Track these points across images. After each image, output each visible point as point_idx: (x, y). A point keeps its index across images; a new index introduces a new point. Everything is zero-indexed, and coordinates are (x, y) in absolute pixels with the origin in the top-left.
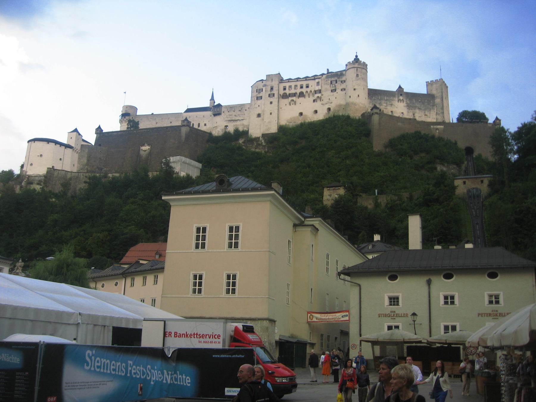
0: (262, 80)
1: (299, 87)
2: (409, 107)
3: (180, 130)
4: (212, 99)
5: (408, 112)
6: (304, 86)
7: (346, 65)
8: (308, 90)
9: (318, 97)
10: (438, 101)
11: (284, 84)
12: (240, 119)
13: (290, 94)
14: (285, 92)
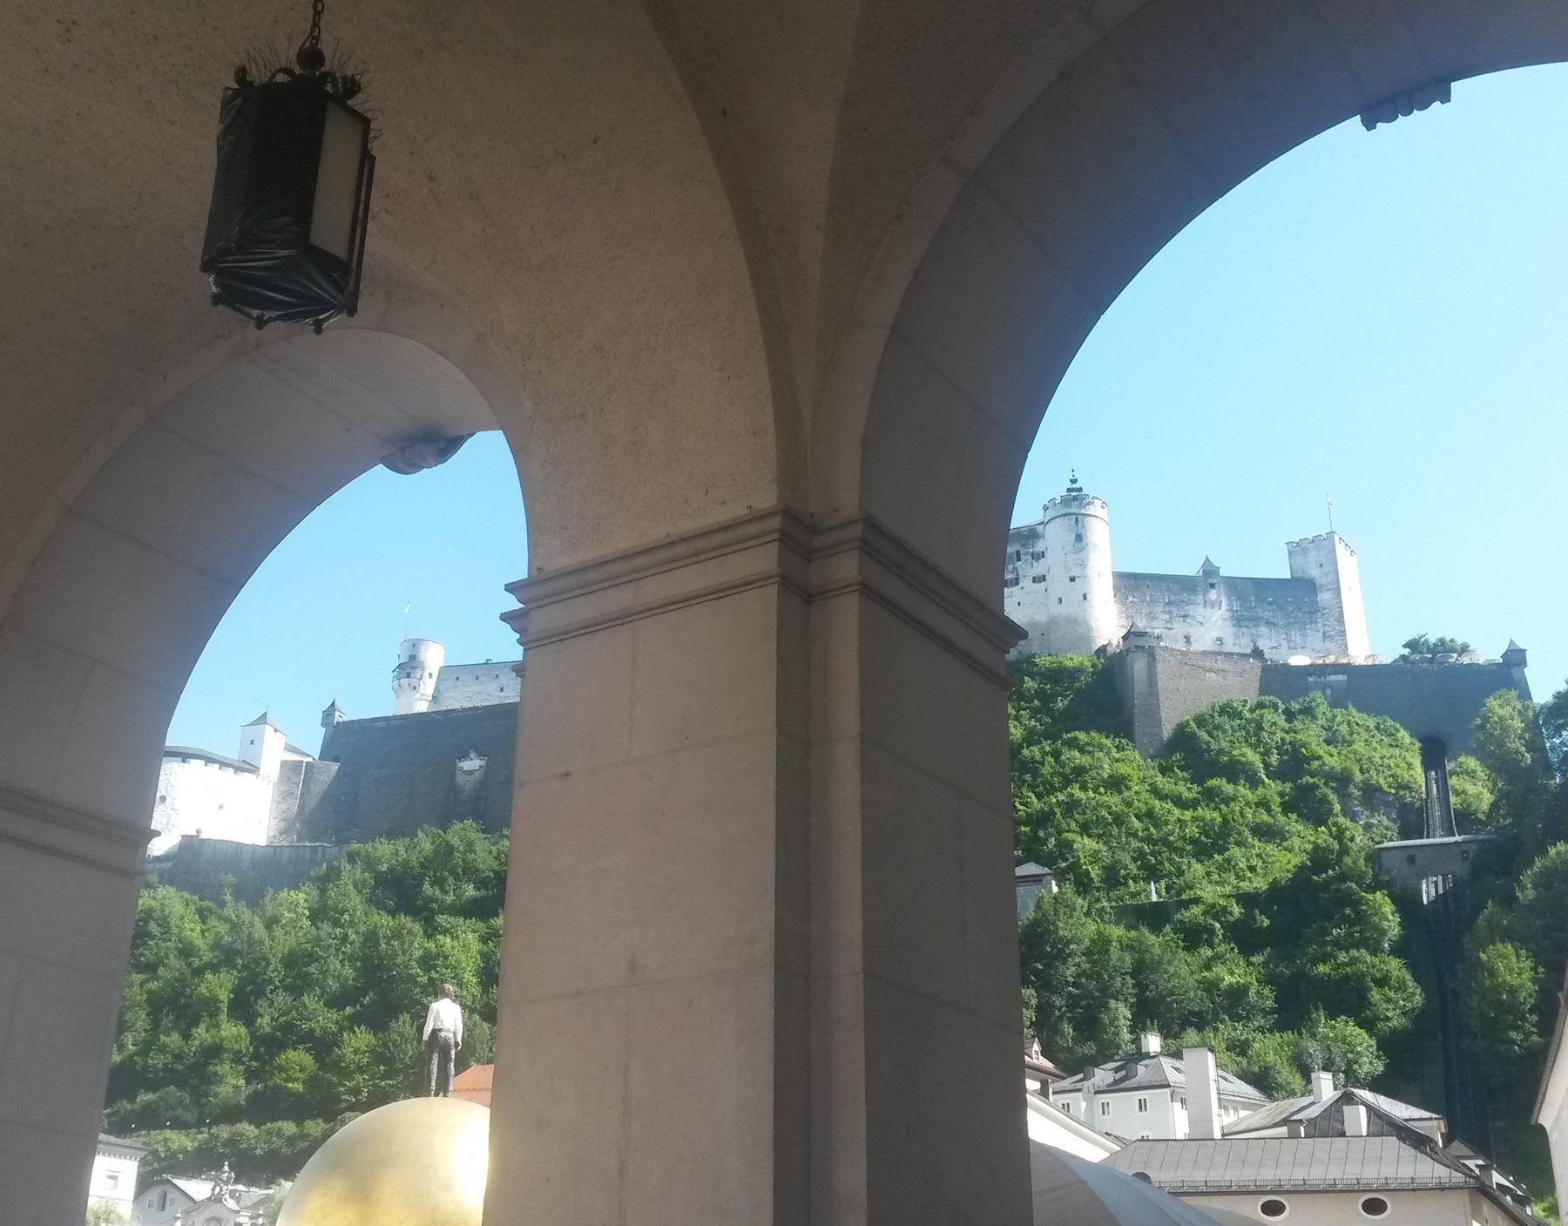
2: (1239, 621)
5: (1237, 636)
7: (1046, 508)
10: (1324, 597)
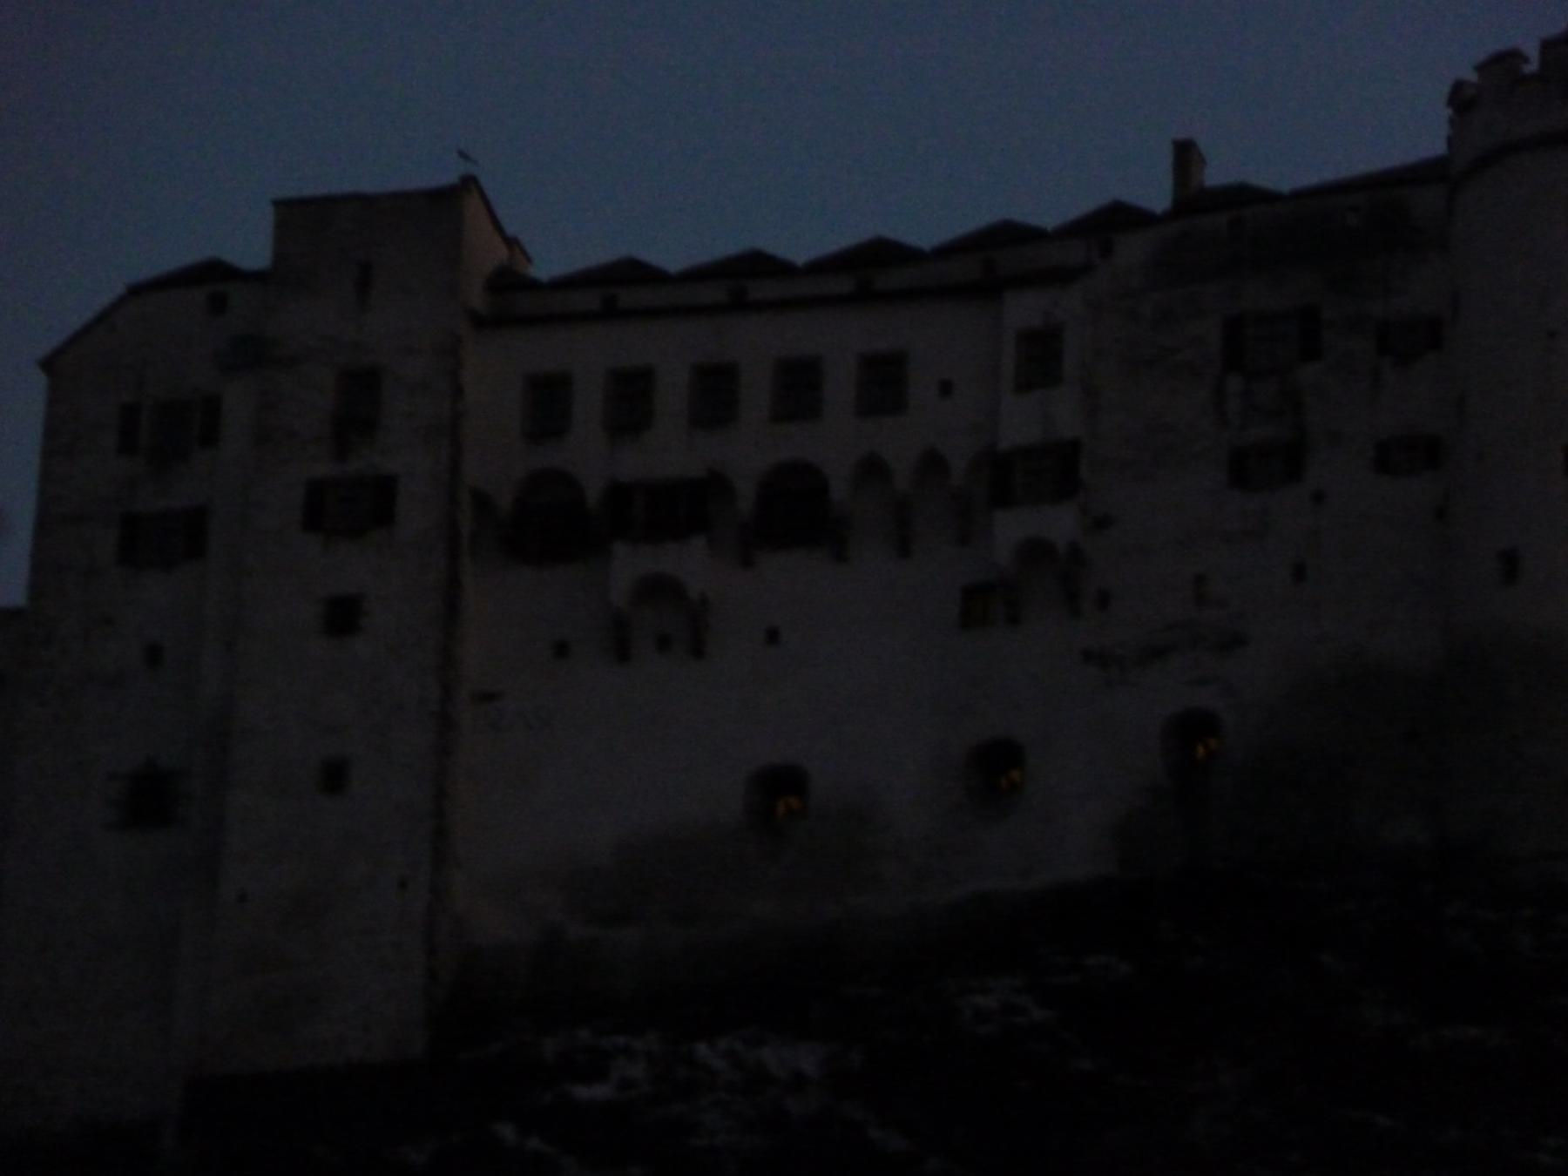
0: (213, 273)
1: (756, 392)
6: (840, 386)
7: (1461, 100)
9: (1036, 552)
13: (619, 493)
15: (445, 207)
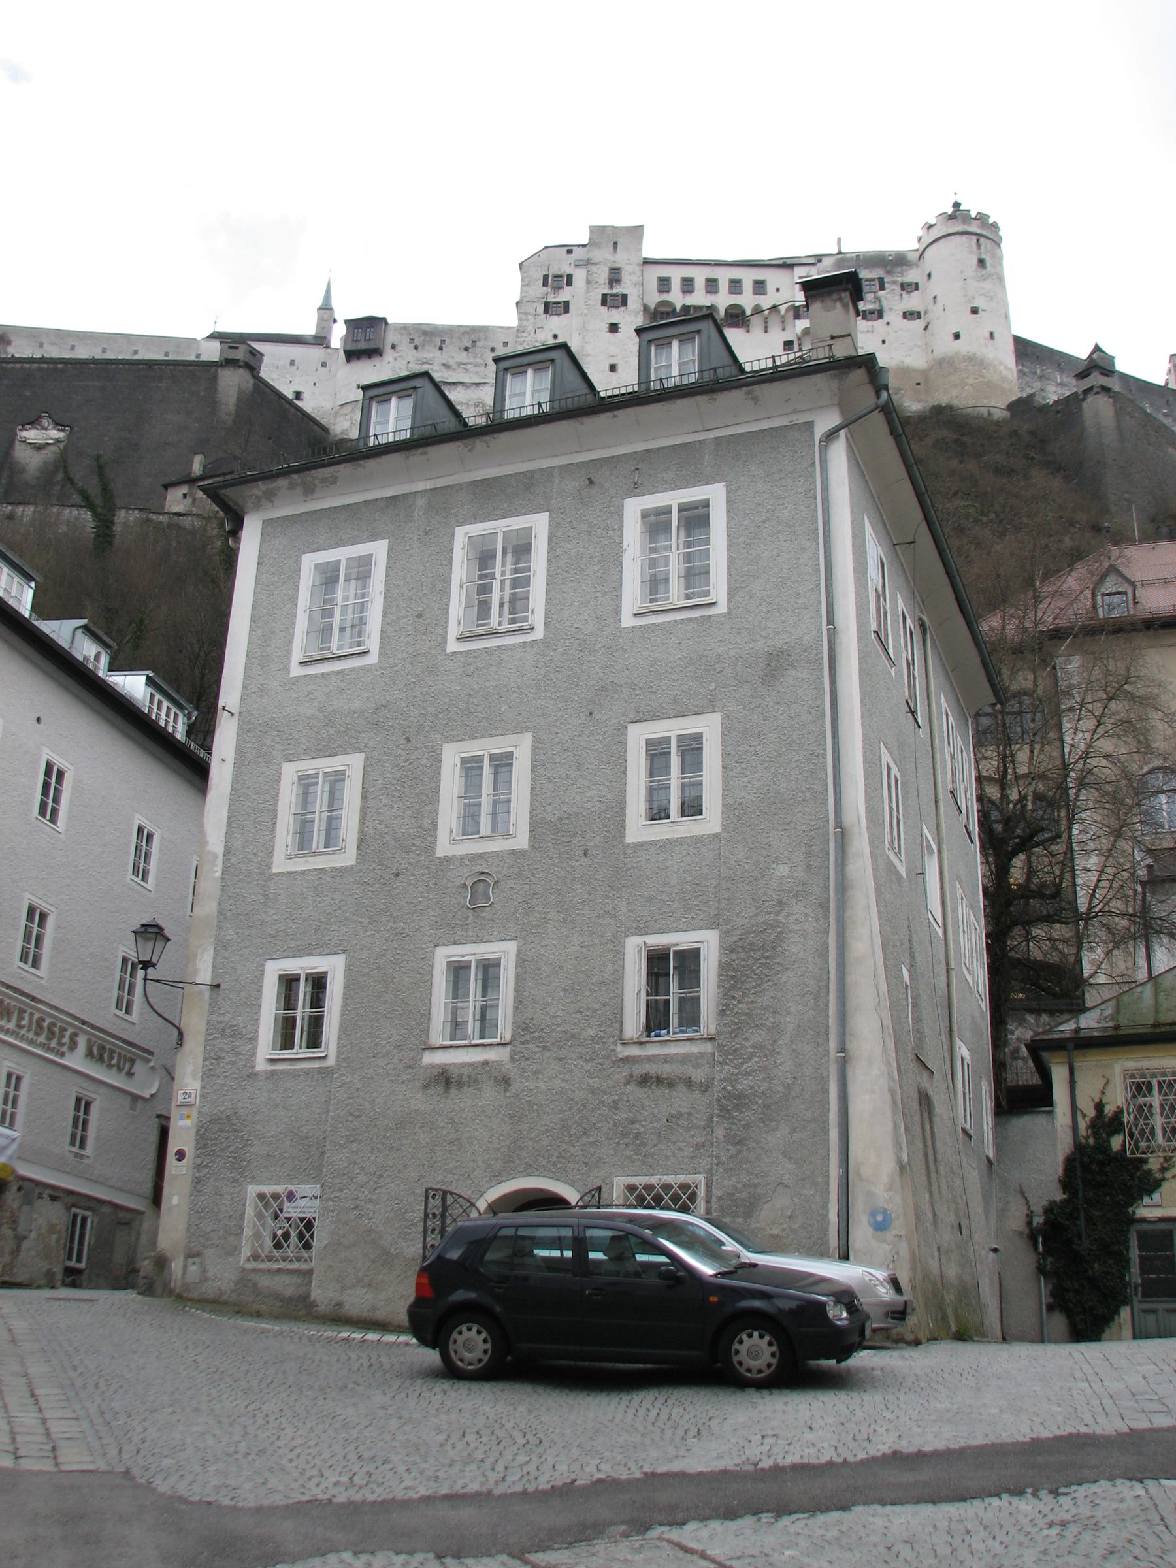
1: (724, 286)
3: (214, 379)
4: (326, 308)
6: (748, 286)
8: (766, 302)
11: (664, 271)
12: (466, 380)
13: (686, 308)
14: (665, 297)
15: (636, 232)
